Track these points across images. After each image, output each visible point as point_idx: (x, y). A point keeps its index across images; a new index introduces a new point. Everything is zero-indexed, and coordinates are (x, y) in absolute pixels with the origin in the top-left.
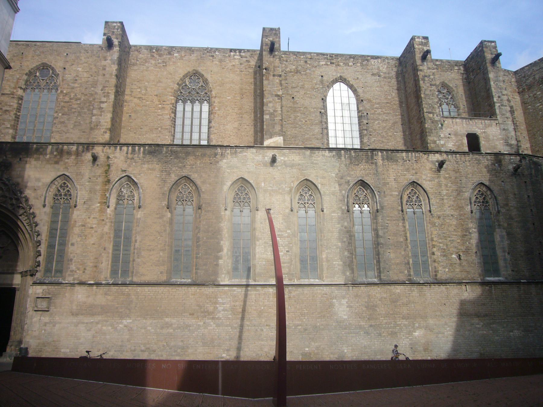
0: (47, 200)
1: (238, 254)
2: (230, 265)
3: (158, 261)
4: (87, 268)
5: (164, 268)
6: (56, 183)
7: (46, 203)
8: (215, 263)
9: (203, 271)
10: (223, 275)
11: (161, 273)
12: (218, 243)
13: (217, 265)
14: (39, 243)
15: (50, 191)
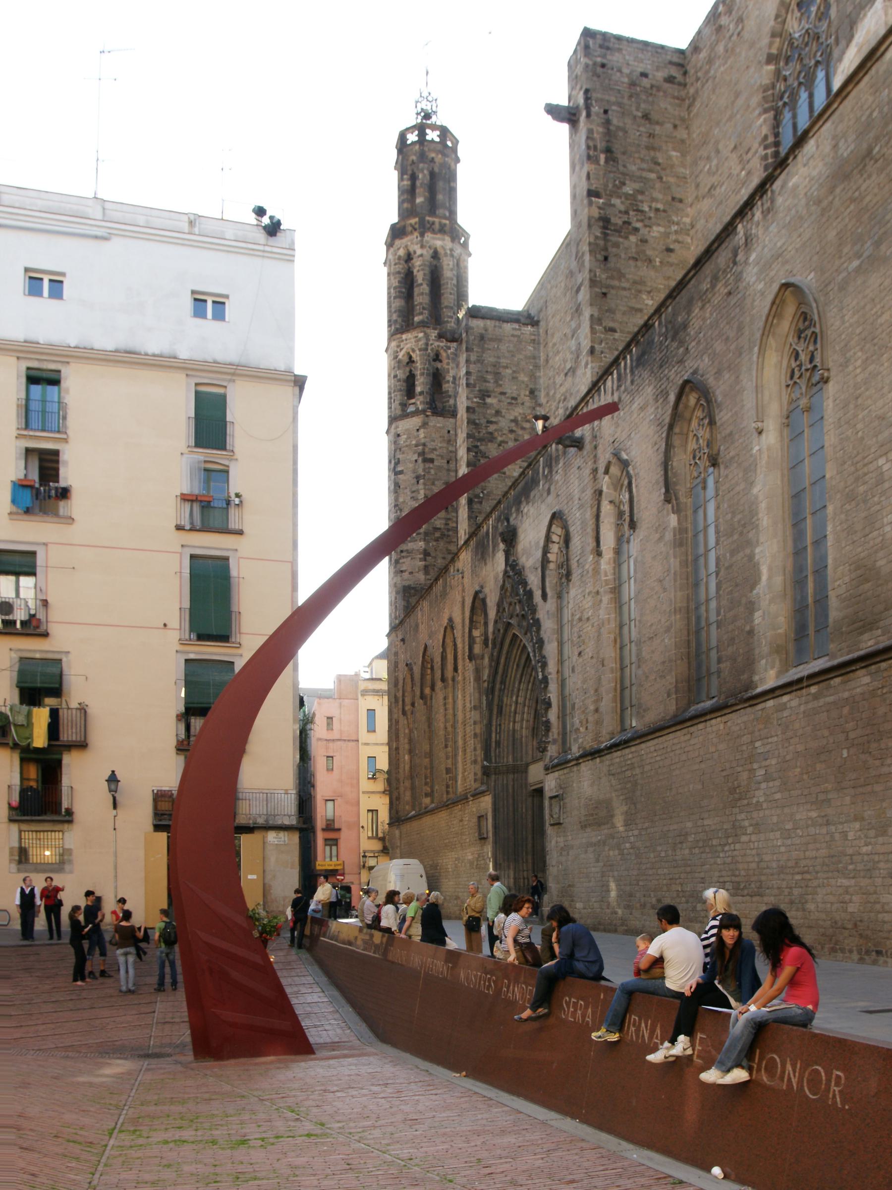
0: (547, 584)
1: (804, 575)
2: (782, 619)
3: (664, 662)
4: (591, 719)
5: (671, 679)
6: (555, 538)
7: (548, 590)
8: (748, 628)
9: (728, 664)
10: (763, 662)
11: (669, 695)
12: (751, 557)
13: (751, 633)
14: (545, 680)
15: (549, 562)
